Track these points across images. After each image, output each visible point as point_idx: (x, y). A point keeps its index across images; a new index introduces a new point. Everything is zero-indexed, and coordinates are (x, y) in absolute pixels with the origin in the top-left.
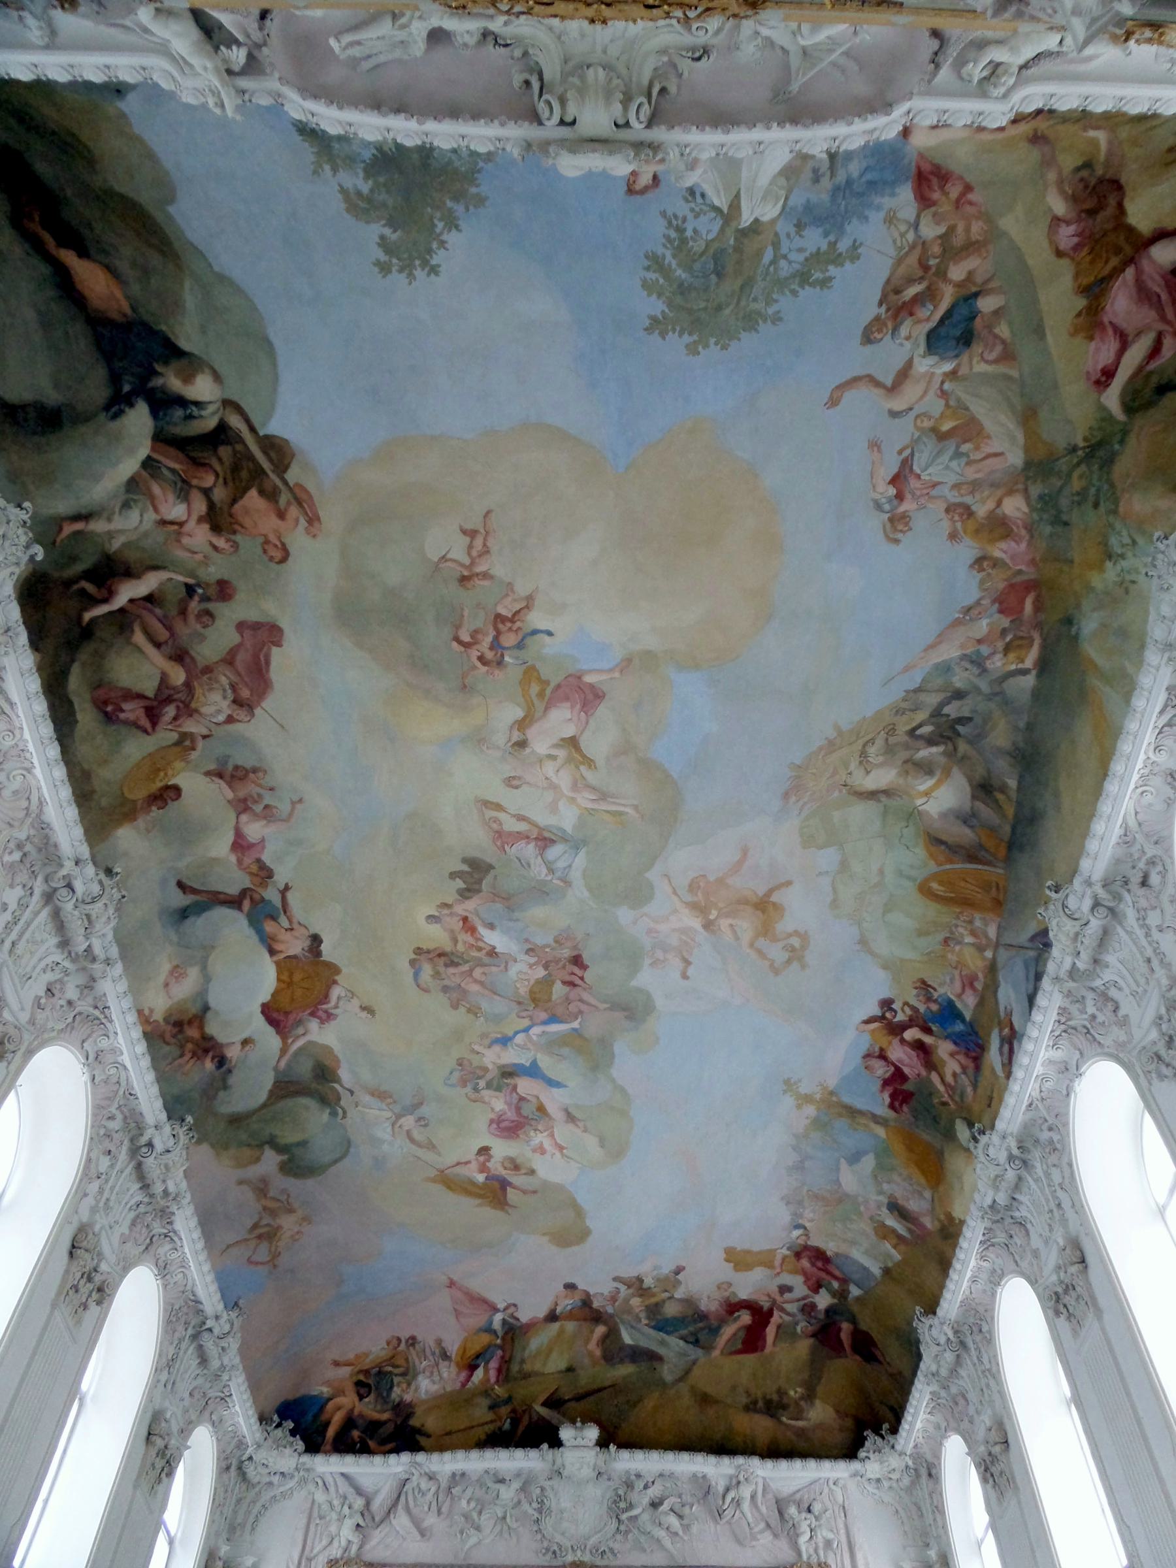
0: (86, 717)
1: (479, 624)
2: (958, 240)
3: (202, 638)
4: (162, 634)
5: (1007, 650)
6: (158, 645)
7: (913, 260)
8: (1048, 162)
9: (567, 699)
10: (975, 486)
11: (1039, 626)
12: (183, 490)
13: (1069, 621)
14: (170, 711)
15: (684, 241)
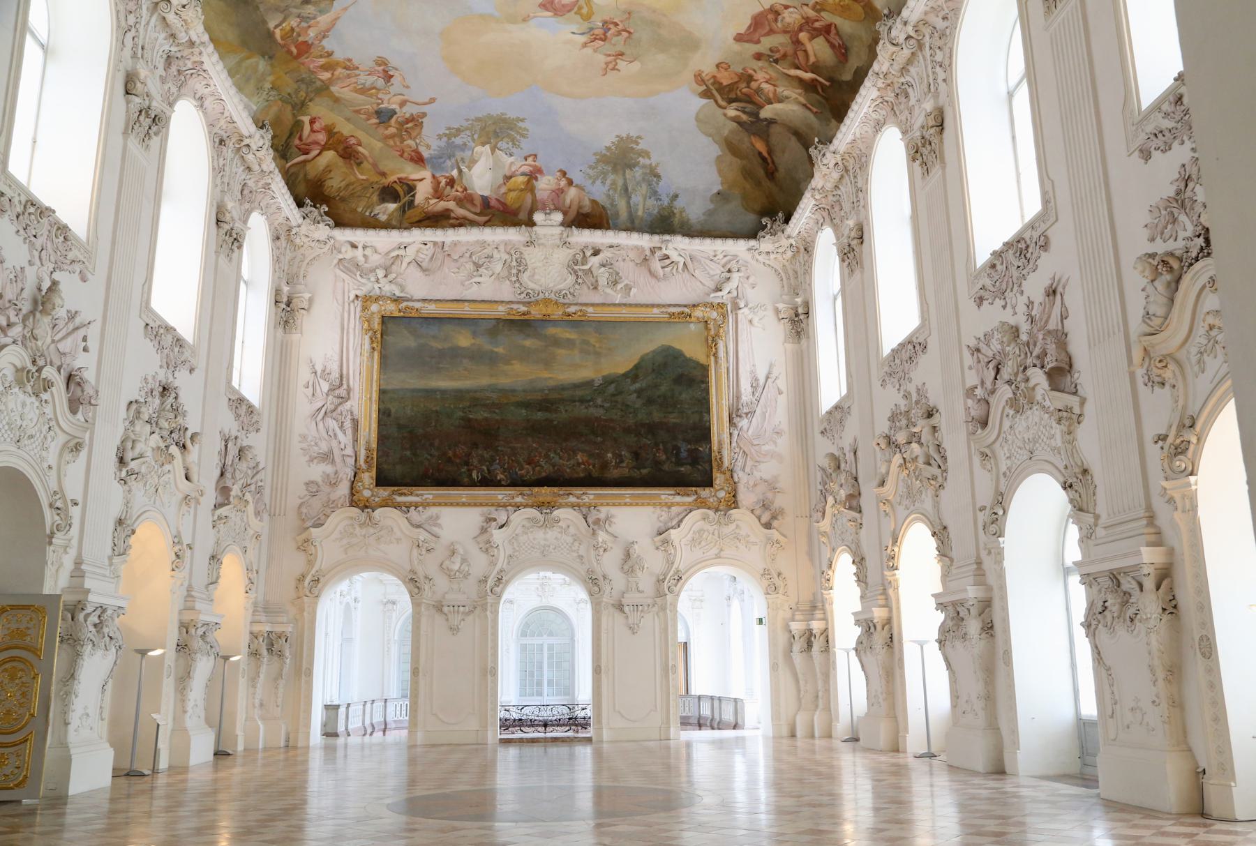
0: (854, 63)
1: (615, 39)
2: (397, 139)
3: (781, 44)
4: (800, 54)
5: (292, 30)
6: (805, 51)
7: (414, 134)
8: (375, 165)
9: (563, 6)
10: (349, 76)
11: (283, 46)
12: (759, 91)
13: (271, 58)
14: (817, 25)
15: (513, 141)
